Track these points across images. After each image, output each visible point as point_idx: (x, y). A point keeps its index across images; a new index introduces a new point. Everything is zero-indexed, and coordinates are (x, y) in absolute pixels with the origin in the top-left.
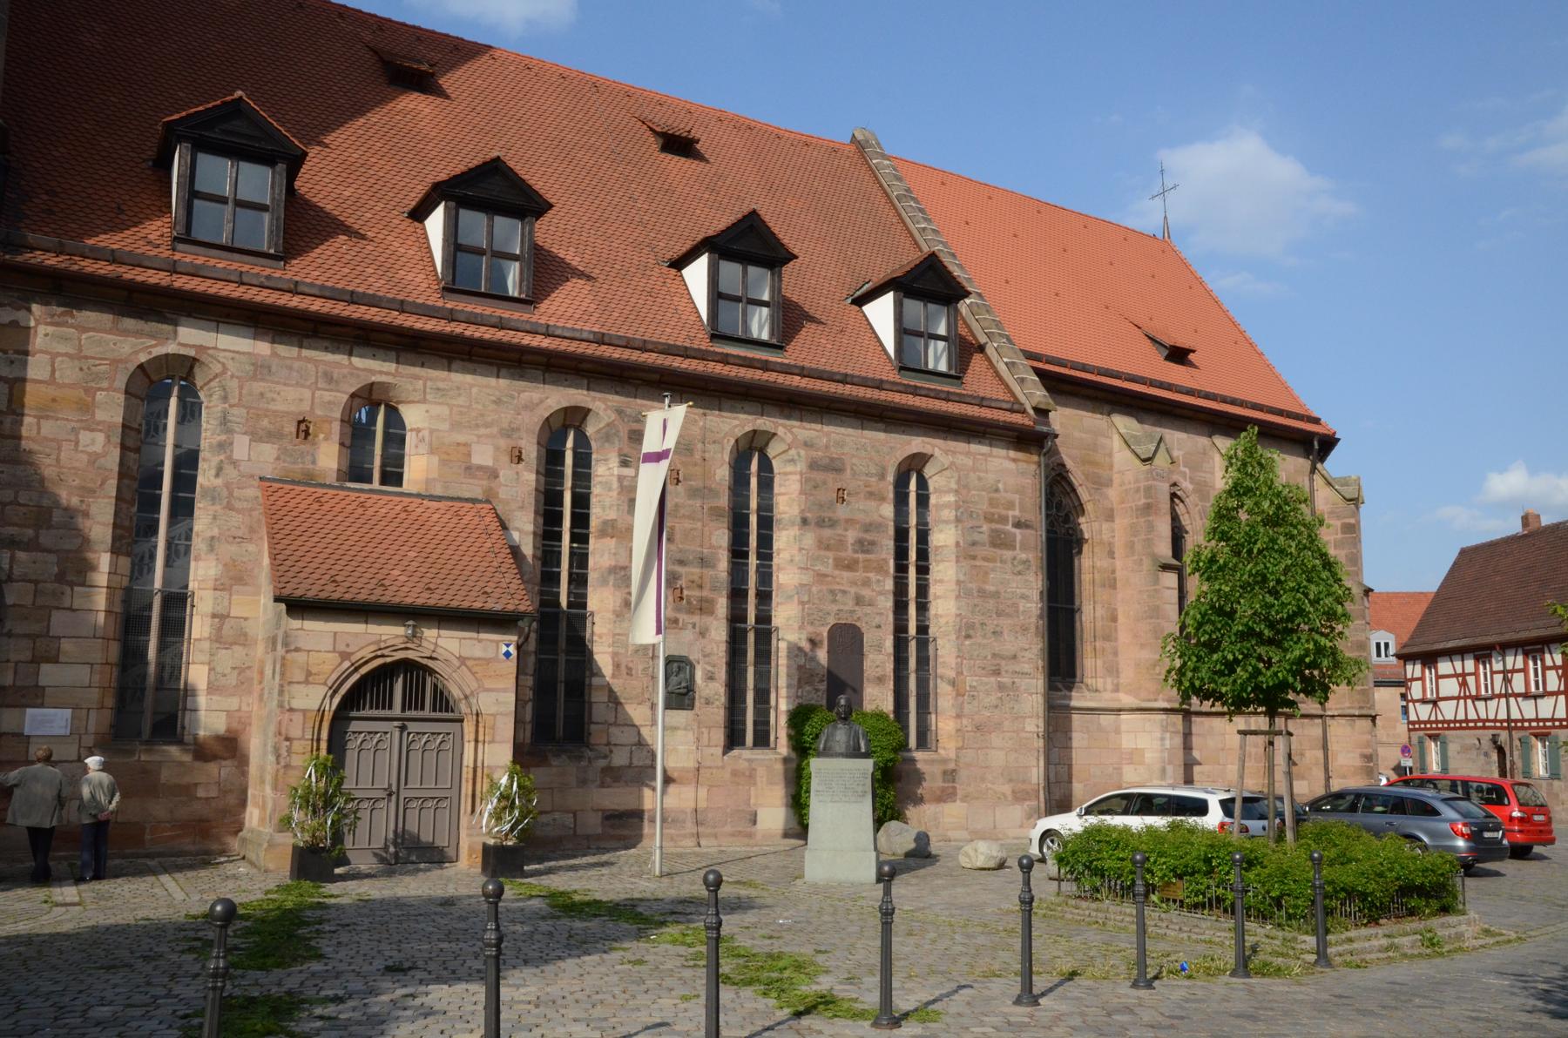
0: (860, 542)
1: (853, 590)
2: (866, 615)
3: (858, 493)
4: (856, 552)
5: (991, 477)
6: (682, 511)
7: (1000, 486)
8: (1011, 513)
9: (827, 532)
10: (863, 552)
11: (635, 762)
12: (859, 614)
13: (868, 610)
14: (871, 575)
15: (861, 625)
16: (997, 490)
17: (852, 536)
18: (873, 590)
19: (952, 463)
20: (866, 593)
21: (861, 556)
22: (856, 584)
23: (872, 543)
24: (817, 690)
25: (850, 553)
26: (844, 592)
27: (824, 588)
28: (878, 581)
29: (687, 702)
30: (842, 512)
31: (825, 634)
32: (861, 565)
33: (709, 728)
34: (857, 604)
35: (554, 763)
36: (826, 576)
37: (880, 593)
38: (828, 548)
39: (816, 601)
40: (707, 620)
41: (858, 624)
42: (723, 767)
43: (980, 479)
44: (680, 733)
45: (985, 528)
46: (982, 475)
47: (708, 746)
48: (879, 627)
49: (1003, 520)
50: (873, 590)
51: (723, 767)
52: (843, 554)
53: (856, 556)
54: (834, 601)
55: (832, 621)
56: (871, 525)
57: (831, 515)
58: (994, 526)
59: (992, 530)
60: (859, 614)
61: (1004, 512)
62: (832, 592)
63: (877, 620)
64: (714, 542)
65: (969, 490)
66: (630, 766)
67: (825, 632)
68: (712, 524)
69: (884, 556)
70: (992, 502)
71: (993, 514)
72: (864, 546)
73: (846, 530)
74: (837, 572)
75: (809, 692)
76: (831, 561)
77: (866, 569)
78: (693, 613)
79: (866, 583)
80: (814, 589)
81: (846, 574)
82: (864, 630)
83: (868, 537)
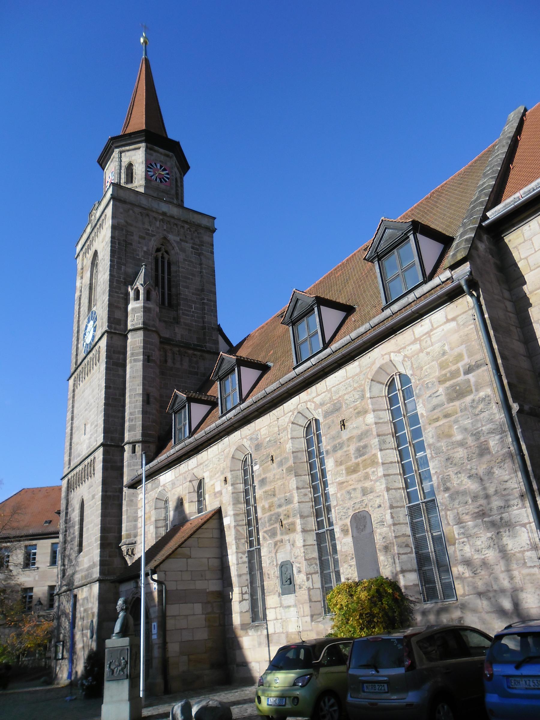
0: (358, 450)
1: (359, 486)
2: (370, 500)
3: (351, 417)
4: (356, 458)
5: (437, 347)
6: (277, 477)
7: (446, 348)
8: (460, 365)
9: (340, 453)
10: (361, 456)
11: (277, 631)
12: (366, 502)
13: (371, 496)
14: (367, 470)
15: (369, 509)
16: (444, 353)
17: (352, 449)
18: (371, 480)
19: (405, 356)
20: (368, 484)
21: (360, 460)
22: (360, 481)
23: (365, 447)
24: (351, 566)
25: (354, 461)
26: (355, 489)
27: (344, 492)
28: (373, 472)
29: (292, 589)
30: (345, 435)
31: (349, 524)
32: (361, 466)
33: (302, 604)
34: (364, 495)
35: (250, 634)
36: (343, 483)
37: (376, 481)
38: (341, 464)
39: (341, 503)
40: (291, 536)
41: (366, 509)
42: (311, 630)
43: (428, 353)
44: (292, 609)
45: (441, 390)
46: (428, 350)
47: (304, 616)
48: (380, 506)
49: (454, 374)
50: (371, 480)
51: (311, 630)
52: (349, 464)
53: (357, 461)
54: (350, 498)
55: (351, 513)
56: (362, 434)
57: (339, 440)
58: (448, 384)
59: (447, 388)
60: (366, 502)
61: (453, 368)
62: (349, 492)
63: (378, 501)
64: (291, 488)
65: (421, 368)
66: (275, 633)
67: (348, 521)
68: (288, 478)
69: (374, 452)
70: (442, 366)
71: (446, 375)
72: (361, 451)
73: (349, 446)
74: (349, 478)
75: (347, 568)
76: (344, 472)
77: (365, 467)
78: (287, 534)
79: (367, 477)
80: (339, 495)
81: (355, 476)
82: (371, 513)
83: (362, 444)
